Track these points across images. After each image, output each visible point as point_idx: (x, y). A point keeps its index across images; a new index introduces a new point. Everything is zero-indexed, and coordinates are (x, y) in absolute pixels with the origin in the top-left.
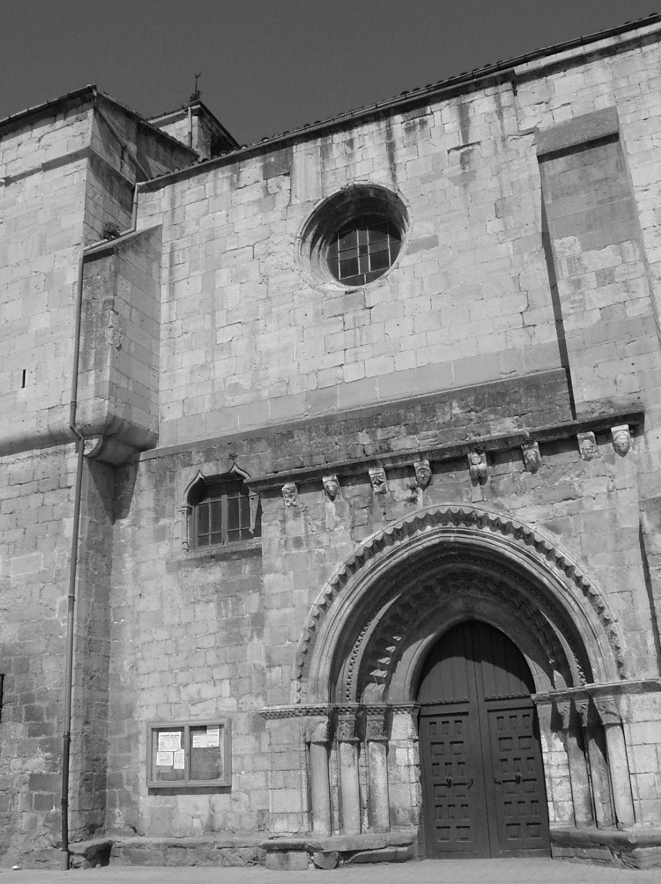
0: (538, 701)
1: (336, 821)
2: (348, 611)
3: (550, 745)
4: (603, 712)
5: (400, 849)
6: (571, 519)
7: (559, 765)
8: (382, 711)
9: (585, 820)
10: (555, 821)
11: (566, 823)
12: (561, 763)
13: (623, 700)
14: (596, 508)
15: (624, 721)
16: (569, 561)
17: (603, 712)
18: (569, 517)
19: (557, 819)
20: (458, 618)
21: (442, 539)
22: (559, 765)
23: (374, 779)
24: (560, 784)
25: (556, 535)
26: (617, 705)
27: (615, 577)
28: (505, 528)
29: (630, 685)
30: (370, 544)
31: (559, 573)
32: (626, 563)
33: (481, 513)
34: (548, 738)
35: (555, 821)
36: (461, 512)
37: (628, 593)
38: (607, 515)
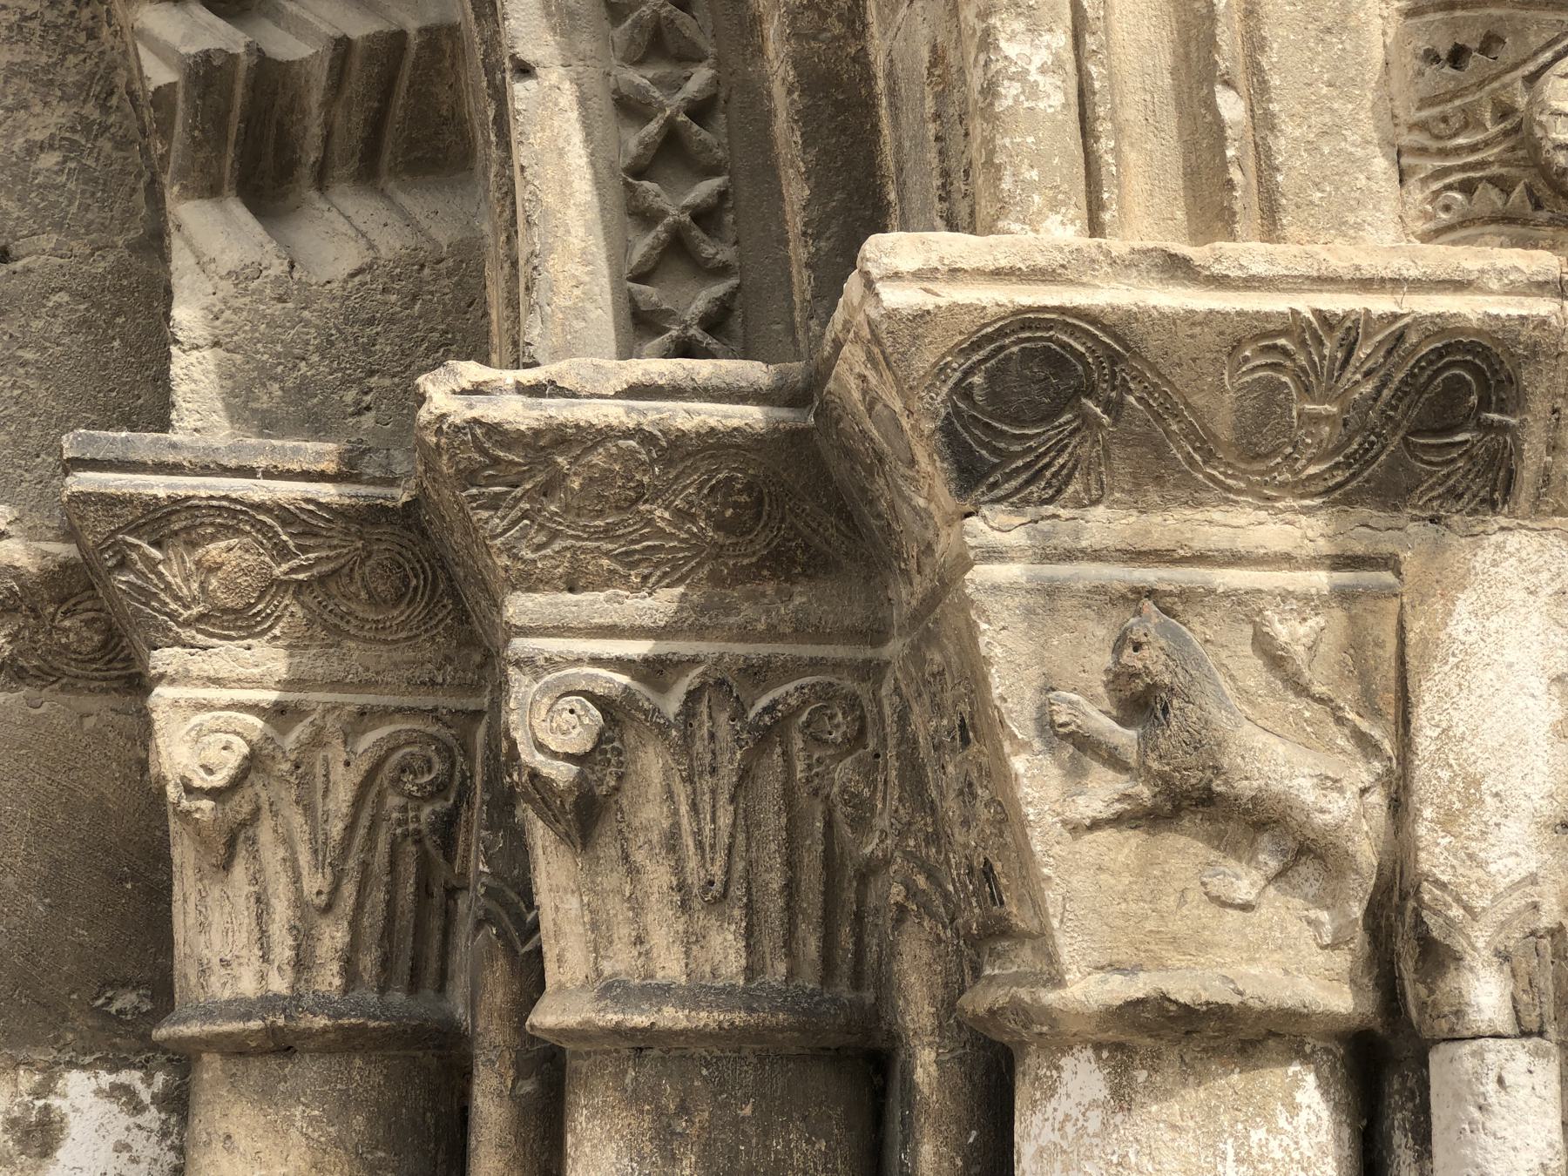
4: (1102, 792)
17: (1102, 792)
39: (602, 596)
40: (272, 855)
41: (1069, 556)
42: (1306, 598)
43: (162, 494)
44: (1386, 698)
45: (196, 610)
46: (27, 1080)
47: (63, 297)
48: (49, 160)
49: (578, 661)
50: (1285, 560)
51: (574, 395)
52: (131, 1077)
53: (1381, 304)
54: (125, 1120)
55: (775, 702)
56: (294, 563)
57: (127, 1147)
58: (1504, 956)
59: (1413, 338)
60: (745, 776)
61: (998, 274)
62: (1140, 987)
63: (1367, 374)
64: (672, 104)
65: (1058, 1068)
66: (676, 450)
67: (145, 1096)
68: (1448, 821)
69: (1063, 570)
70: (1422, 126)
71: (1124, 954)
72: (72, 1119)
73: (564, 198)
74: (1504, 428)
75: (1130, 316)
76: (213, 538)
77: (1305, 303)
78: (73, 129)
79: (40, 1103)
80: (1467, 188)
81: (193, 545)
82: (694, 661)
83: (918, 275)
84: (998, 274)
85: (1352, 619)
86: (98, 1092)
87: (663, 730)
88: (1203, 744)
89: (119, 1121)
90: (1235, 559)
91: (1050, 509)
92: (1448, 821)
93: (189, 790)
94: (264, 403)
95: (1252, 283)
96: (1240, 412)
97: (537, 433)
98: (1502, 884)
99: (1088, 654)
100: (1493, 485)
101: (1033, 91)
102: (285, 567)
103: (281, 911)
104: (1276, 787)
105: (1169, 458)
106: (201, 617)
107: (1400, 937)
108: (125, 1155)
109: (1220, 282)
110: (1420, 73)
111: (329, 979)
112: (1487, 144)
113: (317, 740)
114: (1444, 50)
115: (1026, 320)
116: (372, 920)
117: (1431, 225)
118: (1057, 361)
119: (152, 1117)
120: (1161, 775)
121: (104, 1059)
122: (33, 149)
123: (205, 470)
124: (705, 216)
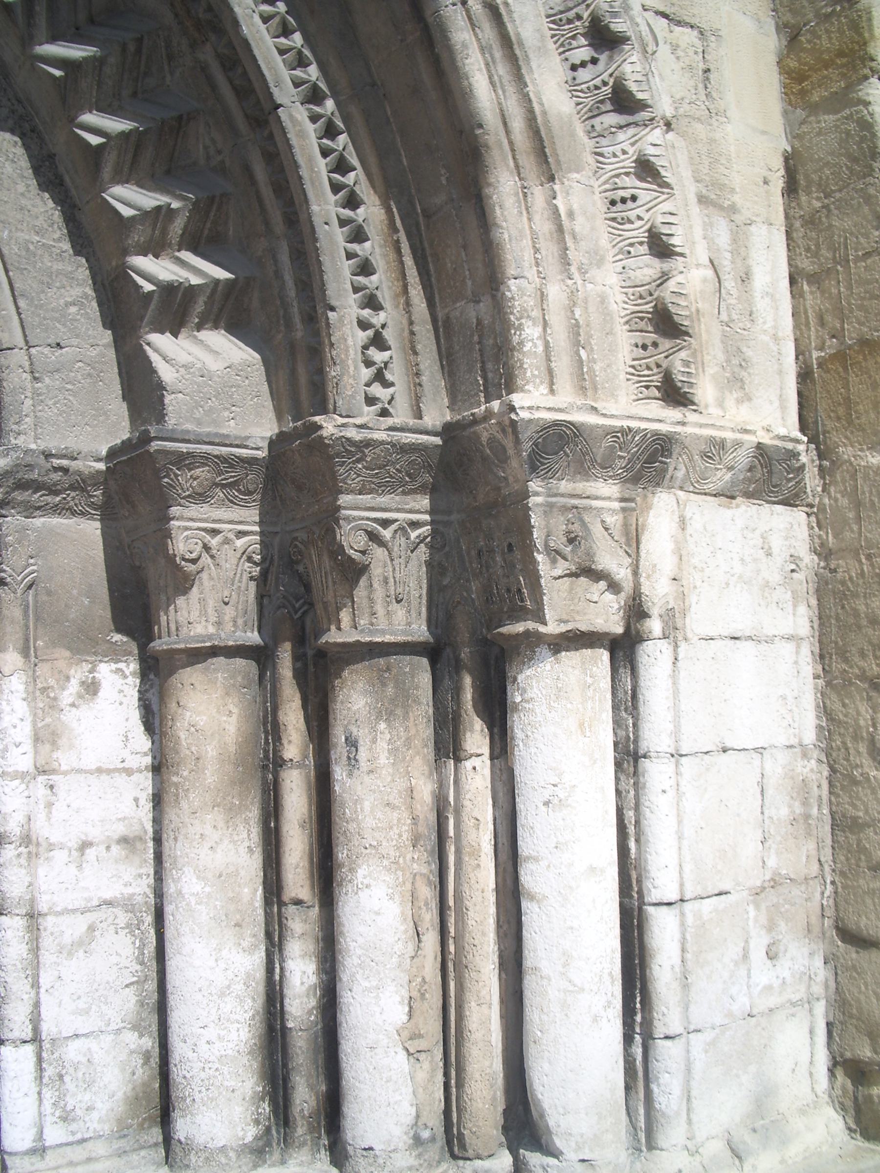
4: (562, 567)
7: (84, 846)
9: (249, 1138)
12: (95, 833)
15: (655, 625)
17: (562, 567)
19: (54, 1135)
22: (84, 846)
24: (86, 941)
39: (369, 496)
41: (555, 495)
42: (614, 511)
43: (185, 451)
44: (633, 539)
45: (187, 493)
46: (86, 667)
47: (80, 364)
48: (73, 309)
49: (363, 519)
50: (609, 498)
51: (371, 429)
52: (122, 665)
53: (643, 425)
54: (122, 681)
55: (420, 535)
56: (223, 477)
57: (122, 691)
58: (661, 616)
59: (649, 435)
61: (549, 409)
62: (569, 626)
63: (637, 446)
65: (534, 652)
66: (405, 449)
67: (127, 672)
69: (554, 499)
70: (633, 367)
71: (565, 617)
72: (103, 681)
73: (347, 356)
74: (665, 463)
75: (583, 424)
76: (199, 467)
77: (625, 423)
78: (82, 297)
79: (91, 675)
80: (647, 387)
81: (190, 470)
82: (396, 520)
83: (529, 408)
84: (549, 409)
85: (625, 517)
86: (111, 671)
88: (590, 555)
90: (597, 498)
91: (551, 481)
92: (648, 577)
93: (184, 559)
94: (197, 415)
95: (612, 416)
96: (604, 454)
97: (361, 442)
98: (661, 595)
99: (559, 524)
101: (535, 346)
102: (220, 478)
104: (607, 567)
105: (584, 467)
106: (189, 496)
107: (636, 611)
108: (122, 694)
109: (604, 415)
110: (632, 351)
111: (229, 627)
112: (653, 375)
113: (227, 541)
114: (640, 345)
115: (556, 424)
117: (635, 397)
118: (561, 436)
119: (130, 680)
120: (578, 562)
121: (112, 659)
122: (68, 304)
123: (199, 443)
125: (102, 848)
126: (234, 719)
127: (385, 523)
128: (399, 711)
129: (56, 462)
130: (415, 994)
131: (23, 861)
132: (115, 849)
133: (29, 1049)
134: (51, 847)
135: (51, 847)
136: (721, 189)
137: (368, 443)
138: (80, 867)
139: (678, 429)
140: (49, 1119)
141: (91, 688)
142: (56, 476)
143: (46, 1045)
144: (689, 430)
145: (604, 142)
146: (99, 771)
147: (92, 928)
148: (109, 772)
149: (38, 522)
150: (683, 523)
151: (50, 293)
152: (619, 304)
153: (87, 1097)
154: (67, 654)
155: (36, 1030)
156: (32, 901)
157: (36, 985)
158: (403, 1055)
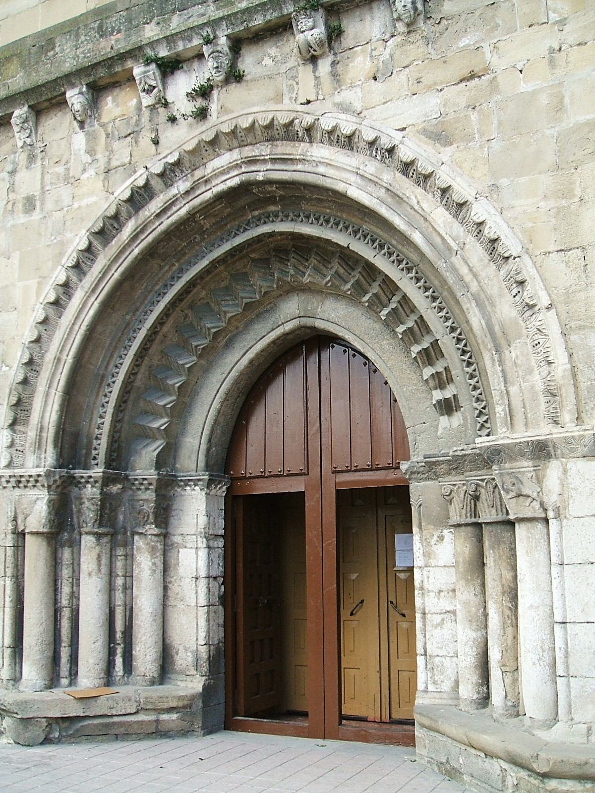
0: (412, 473)
1: (60, 664)
2: (92, 313)
3: (427, 555)
5: (164, 717)
6: (474, 116)
7: (440, 591)
8: (150, 484)
9: (474, 698)
10: (426, 691)
11: (445, 696)
12: (443, 588)
13: (553, 470)
14: (524, 87)
15: (551, 514)
16: (462, 190)
17: (512, 494)
18: (470, 111)
19: (431, 688)
20: (288, 327)
21: (244, 177)
22: (440, 591)
23: (137, 596)
25: (442, 149)
26: (539, 481)
27: (553, 220)
28: (349, 142)
29: (567, 441)
30: (127, 194)
31: (440, 217)
32: (578, 192)
33: (308, 120)
34: (425, 542)
35: (426, 691)
36: (276, 123)
37: (579, 252)
38: (544, 100)
40: (456, 502)
48: (428, 409)
60: (494, 492)
64: (480, 408)
68: (547, 495)
87: (483, 487)
89: (451, 536)
99: (508, 480)
100: (549, 456)
103: (457, 509)
113: (459, 487)
116: (468, 510)
124: (486, 422)
125: (446, 593)
126: (468, 549)
127: (482, 480)
128: (496, 546)
129: (420, 464)
130: (504, 649)
131: (420, 595)
132: (450, 593)
133: (423, 657)
134: (429, 592)
135: (429, 592)
136: (592, 319)
137: (465, 455)
138: (439, 599)
139: (549, 437)
140: (429, 682)
141: (441, 538)
142: (422, 469)
143: (428, 657)
144: (554, 436)
145: (528, 323)
146: (445, 566)
147: (443, 620)
148: (448, 567)
149: (422, 484)
150: (565, 471)
151: (421, 405)
152: (540, 386)
153: (442, 677)
154: (433, 527)
155: (425, 651)
156: (424, 609)
157: (425, 637)
158: (500, 672)
